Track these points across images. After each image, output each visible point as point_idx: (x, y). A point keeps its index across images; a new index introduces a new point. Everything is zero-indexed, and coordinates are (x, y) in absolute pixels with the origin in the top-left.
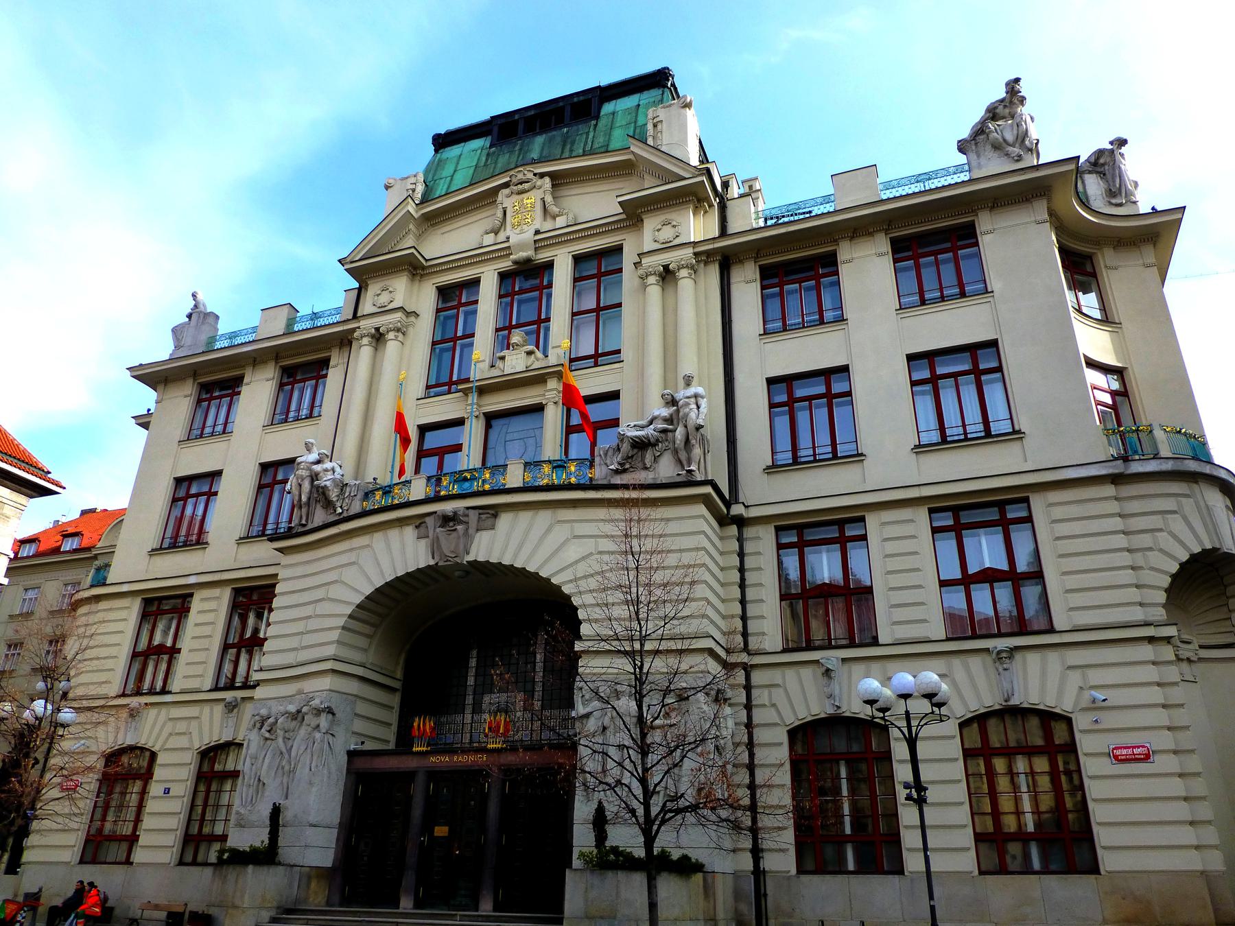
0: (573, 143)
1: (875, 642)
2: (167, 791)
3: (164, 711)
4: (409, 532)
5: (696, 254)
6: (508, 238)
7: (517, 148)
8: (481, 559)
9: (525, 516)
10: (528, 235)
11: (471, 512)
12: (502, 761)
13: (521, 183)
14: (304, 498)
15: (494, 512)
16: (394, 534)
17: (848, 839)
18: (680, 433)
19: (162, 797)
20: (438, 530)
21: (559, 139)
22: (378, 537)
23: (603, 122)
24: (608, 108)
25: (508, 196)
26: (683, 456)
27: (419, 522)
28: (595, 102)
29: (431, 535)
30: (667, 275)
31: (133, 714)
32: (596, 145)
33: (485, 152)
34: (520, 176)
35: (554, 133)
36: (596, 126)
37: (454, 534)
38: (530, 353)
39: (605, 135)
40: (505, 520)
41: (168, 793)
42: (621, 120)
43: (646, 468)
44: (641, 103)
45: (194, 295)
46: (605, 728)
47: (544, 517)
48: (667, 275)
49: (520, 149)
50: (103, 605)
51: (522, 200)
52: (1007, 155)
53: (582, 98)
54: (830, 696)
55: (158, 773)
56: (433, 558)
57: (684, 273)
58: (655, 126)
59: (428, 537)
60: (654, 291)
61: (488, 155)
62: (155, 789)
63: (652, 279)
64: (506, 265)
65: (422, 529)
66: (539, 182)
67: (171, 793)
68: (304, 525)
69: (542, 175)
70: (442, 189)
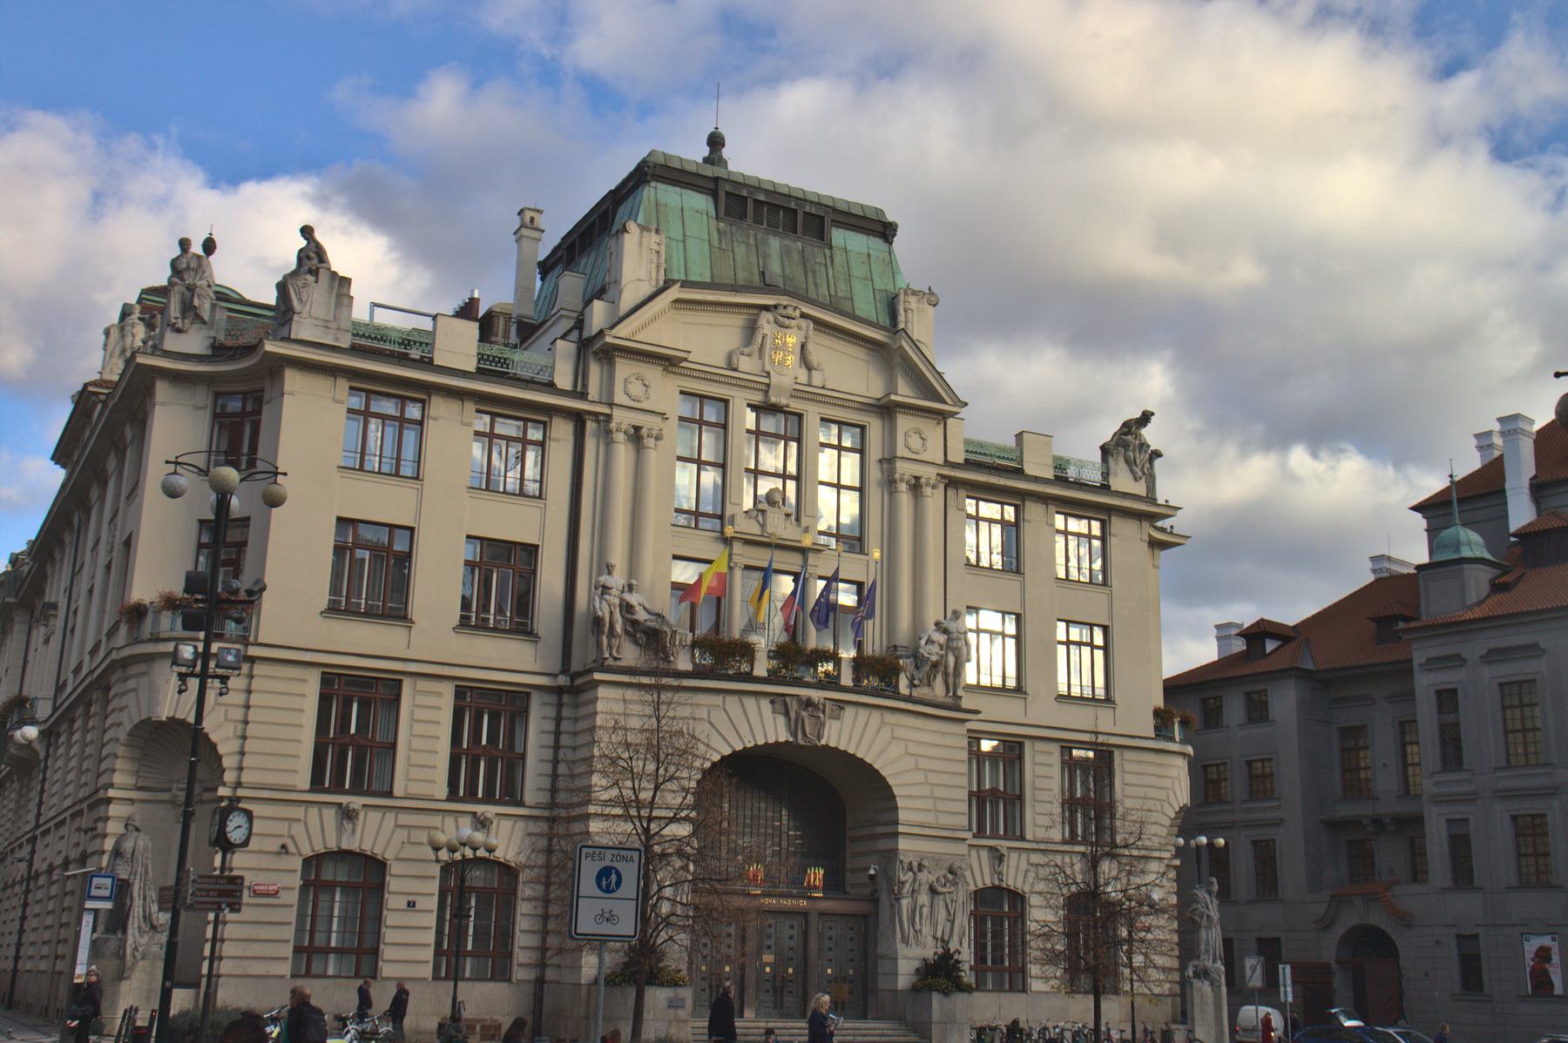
0: (814, 273)
1: (1022, 838)
2: (411, 904)
3: (390, 817)
4: (765, 704)
5: (938, 474)
6: (768, 373)
7: (752, 242)
8: (832, 744)
9: (863, 713)
10: (787, 381)
11: (828, 703)
12: (818, 907)
13: (788, 318)
14: (619, 628)
15: (841, 705)
16: (750, 703)
17: (988, 969)
18: (951, 660)
19: (403, 910)
20: (804, 714)
21: (796, 257)
22: (732, 701)
23: (839, 258)
24: (839, 236)
25: (768, 322)
26: (951, 680)
27: (774, 698)
28: (827, 221)
29: (793, 715)
30: (916, 486)
31: (348, 815)
32: (840, 294)
33: (713, 222)
34: (790, 311)
35: (787, 242)
36: (831, 257)
37: (813, 719)
38: (788, 515)
39: (845, 280)
40: (849, 712)
41: (414, 906)
42: (858, 270)
43: (929, 685)
44: (871, 252)
45: (307, 232)
46: (913, 891)
47: (876, 715)
48: (916, 486)
49: (757, 246)
50: (259, 669)
51: (785, 335)
52: (1132, 471)
53: (813, 211)
54: (1000, 873)
55: (393, 884)
56: (795, 735)
57: (928, 491)
58: (905, 311)
59: (787, 714)
60: (905, 499)
61: (718, 230)
62: (393, 901)
63: (903, 487)
64: (757, 398)
65: (779, 706)
66: (803, 323)
67: (418, 907)
68: (616, 659)
69: (803, 316)
70: (678, 260)
